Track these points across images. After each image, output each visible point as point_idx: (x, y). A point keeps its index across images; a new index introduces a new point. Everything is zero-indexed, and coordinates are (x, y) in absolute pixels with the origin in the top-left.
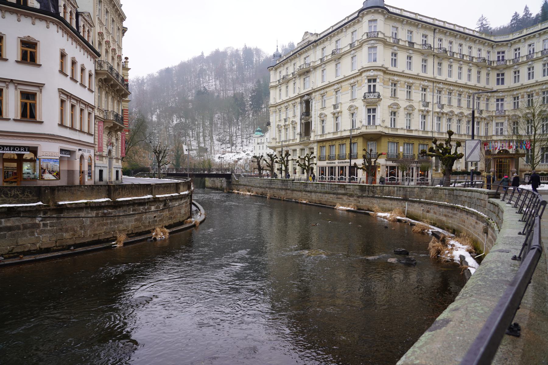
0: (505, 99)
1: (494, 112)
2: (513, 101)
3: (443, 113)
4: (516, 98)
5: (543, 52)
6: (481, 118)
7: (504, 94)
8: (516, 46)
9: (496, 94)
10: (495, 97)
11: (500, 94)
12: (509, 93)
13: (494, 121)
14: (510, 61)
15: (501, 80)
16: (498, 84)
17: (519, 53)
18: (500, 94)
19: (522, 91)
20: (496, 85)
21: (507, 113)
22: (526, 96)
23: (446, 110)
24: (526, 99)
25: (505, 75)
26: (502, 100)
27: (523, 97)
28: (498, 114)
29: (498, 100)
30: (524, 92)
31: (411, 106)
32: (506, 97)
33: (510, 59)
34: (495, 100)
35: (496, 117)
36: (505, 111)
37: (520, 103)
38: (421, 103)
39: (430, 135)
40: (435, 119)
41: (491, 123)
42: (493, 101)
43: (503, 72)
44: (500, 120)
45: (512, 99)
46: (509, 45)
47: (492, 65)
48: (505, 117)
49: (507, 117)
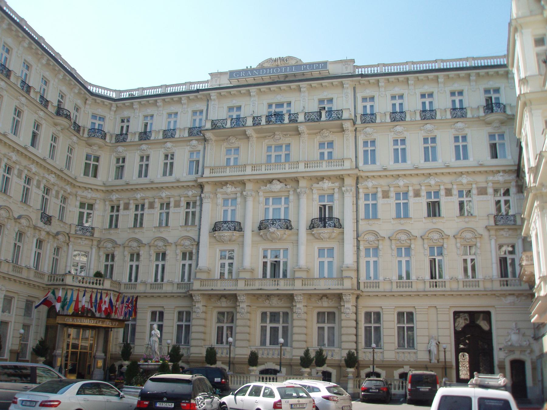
0: (96, 206)
5: (166, 132)
6: (48, 233)
8: (126, 113)
9: (80, 192)
13: (71, 246)
14: (111, 136)
16: (86, 174)
17: (128, 127)
18: (89, 195)
20: (82, 175)
24: (132, 212)
29: (82, 205)
32: (98, 201)
33: (111, 132)
34: (78, 204)
41: (65, 249)
43: (98, 154)
46: (114, 109)
47: (81, 134)
49: (95, 243)
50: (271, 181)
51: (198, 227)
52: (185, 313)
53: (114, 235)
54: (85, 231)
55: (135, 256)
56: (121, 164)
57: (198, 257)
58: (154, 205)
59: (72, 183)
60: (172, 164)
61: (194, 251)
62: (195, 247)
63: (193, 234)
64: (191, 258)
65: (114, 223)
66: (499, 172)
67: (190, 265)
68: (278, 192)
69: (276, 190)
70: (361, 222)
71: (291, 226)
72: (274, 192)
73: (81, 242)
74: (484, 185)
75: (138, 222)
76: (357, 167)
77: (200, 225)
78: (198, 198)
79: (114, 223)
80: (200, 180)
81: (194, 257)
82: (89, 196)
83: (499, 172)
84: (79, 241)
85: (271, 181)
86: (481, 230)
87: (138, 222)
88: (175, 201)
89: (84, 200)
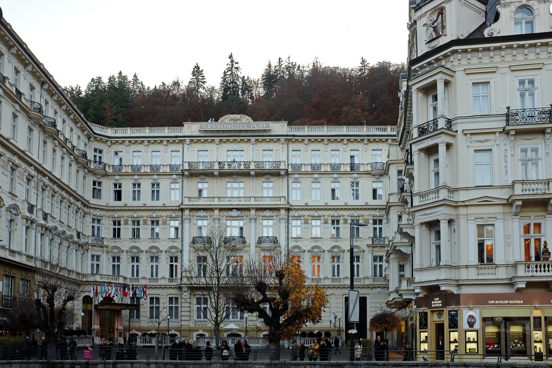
0: (103, 221)
1: (90, 238)
2: (112, 227)
3: (47, 229)
4: (117, 223)
7: (103, 213)
9: (92, 211)
10: (92, 216)
11: (98, 213)
12: (108, 214)
15: (97, 193)
19: (126, 214)
21: (105, 243)
22: (130, 222)
23: (50, 224)
24: (130, 227)
25: (103, 185)
26: (99, 221)
27: (126, 223)
28: (94, 242)
30: (128, 217)
31: (15, 207)
32: (104, 218)
34: (91, 220)
35: (92, 246)
36: (103, 238)
37: (141, 231)
38: (26, 206)
39: (32, 264)
40: (39, 235)
42: (89, 219)
44: (97, 251)
45: (112, 223)
48: (102, 247)
50: (231, 209)
51: (180, 239)
52: (174, 298)
53: (118, 243)
54: (97, 240)
55: (135, 259)
56: (118, 189)
57: (182, 261)
58: (147, 222)
59: (86, 204)
60: (158, 191)
61: (179, 257)
62: (179, 253)
63: (178, 244)
64: (176, 261)
65: (117, 234)
66: (376, 209)
67: (176, 266)
68: (236, 217)
69: (235, 216)
70: (290, 240)
71: (245, 241)
72: (234, 217)
73: (96, 248)
74: (367, 217)
75: (136, 234)
76: (288, 203)
77: (182, 238)
78: (180, 219)
79: (117, 234)
80: (182, 207)
81: (179, 260)
82: (98, 214)
83: (376, 209)
84: (95, 248)
85: (231, 209)
86: (364, 247)
87: (136, 234)
88: (163, 220)
89: (95, 217)
